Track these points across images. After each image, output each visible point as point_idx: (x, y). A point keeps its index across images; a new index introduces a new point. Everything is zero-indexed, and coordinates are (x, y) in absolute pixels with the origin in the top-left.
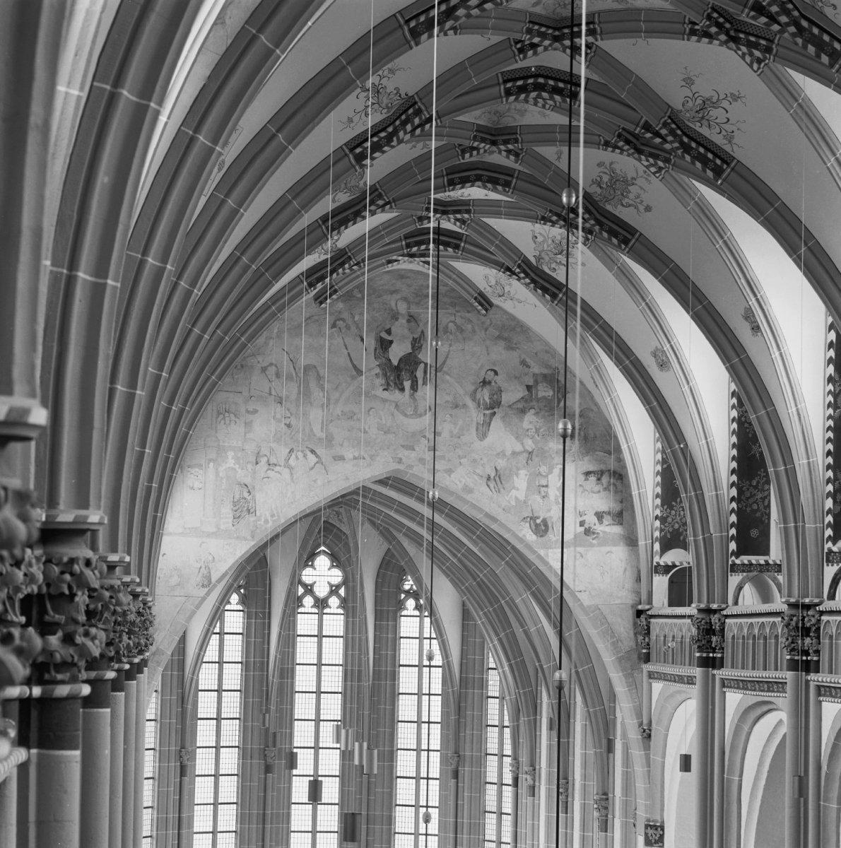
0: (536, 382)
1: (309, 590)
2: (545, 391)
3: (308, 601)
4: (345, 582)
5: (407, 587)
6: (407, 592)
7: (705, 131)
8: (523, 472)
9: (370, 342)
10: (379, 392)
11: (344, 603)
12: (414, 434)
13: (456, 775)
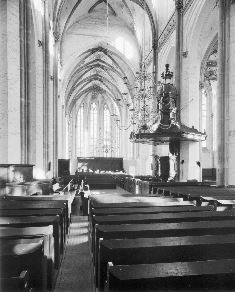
1: (92, 107)
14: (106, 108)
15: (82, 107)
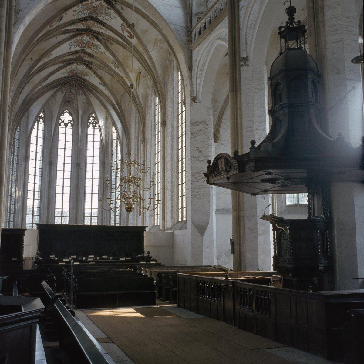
1: (63, 121)
3: (62, 124)
4: (72, 120)
5: (90, 121)
6: (90, 123)
11: (72, 125)
14: (92, 123)
15: (41, 120)
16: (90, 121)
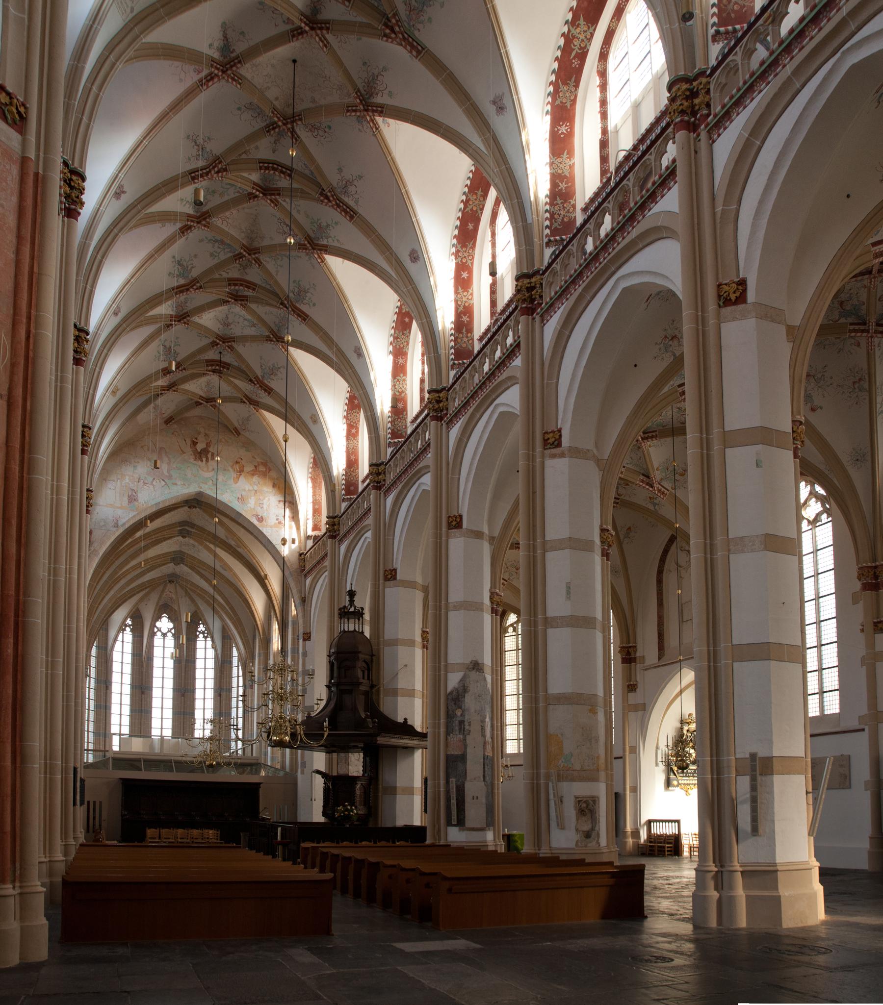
0: (259, 465)
1: (159, 630)
2: (262, 468)
3: (159, 634)
4: (174, 628)
6: (200, 632)
7: (346, 199)
8: (253, 498)
9: (189, 442)
10: (192, 460)
11: (174, 635)
12: (207, 478)
13: (220, 695)
14: (203, 633)
15: (128, 629)
16: (199, 630)
